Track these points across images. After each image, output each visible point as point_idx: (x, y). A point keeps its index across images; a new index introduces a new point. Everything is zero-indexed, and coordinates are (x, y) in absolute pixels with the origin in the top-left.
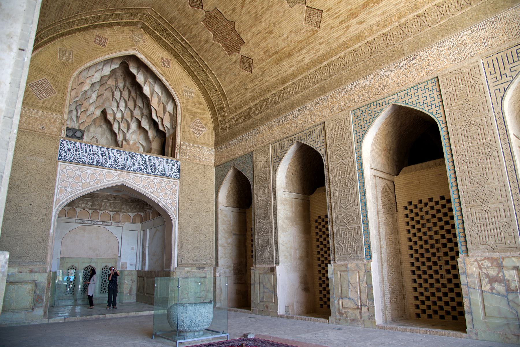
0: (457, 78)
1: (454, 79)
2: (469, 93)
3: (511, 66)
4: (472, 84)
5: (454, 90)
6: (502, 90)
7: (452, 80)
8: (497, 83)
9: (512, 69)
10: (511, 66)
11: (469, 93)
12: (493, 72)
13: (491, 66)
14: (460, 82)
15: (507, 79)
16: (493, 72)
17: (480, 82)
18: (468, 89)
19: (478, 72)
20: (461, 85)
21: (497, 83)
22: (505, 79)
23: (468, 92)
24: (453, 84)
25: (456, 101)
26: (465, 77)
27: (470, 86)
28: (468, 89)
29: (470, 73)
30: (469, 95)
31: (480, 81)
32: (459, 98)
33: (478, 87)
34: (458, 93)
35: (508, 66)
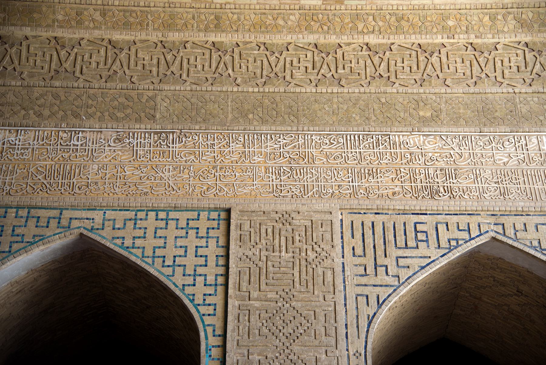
0: (277, 232)
1: (270, 230)
2: (297, 279)
3: (400, 253)
4: (310, 260)
5: (264, 258)
6: (373, 301)
7: (263, 231)
8: (364, 280)
9: (402, 262)
10: (400, 253)
11: (297, 279)
12: (359, 251)
13: (358, 235)
14: (283, 243)
15: (386, 278)
16: (359, 251)
17: (328, 263)
18: (297, 269)
19: (328, 236)
20: (283, 254)
21: (364, 280)
22: (382, 278)
23: (297, 274)
24: (263, 241)
25: (263, 287)
26: (297, 238)
27: (303, 263)
28: (297, 269)
29: (309, 233)
30: (297, 285)
31: (330, 261)
32: (271, 281)
33: (321, 273)
34: (271, 269)
35: (393, 252)
